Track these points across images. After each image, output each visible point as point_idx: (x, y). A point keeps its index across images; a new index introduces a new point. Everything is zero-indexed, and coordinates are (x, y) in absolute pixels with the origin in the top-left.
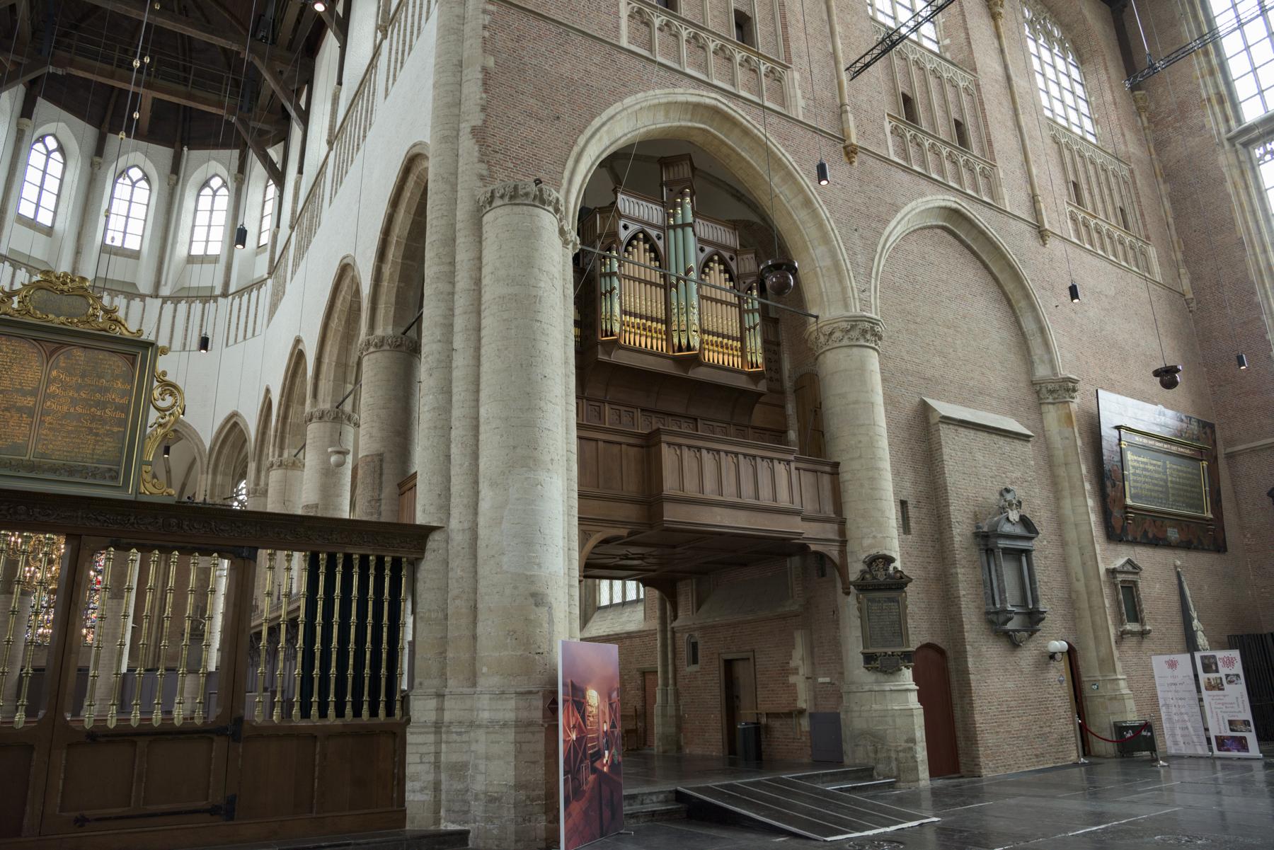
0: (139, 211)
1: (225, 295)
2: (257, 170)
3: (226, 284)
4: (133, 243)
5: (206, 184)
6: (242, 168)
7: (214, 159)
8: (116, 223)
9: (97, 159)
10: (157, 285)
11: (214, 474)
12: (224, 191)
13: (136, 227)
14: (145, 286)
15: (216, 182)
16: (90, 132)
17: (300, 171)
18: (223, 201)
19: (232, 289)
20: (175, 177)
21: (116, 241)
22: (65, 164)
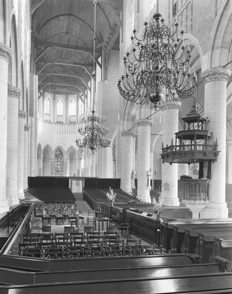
0: (62, 108)
1: (77, 123)
2: (80, 101)
3: (77, 122)
4: (61, 114)
5: (72, 101)
6: (78, 99)
7: (73, 97)
8: (58, 111)
9: (54, 100)
10: (66, 122)
11: (79, 155)
12: (75, 102)
13: (62, 111)
14: (64, 122)
15: (73, 101)
16: (52, 95)
17: (87, 108)
18: (75, 104)
19: (78, 122)
20: (67, 101)
21: (58, 114)
22: (49, 101)
